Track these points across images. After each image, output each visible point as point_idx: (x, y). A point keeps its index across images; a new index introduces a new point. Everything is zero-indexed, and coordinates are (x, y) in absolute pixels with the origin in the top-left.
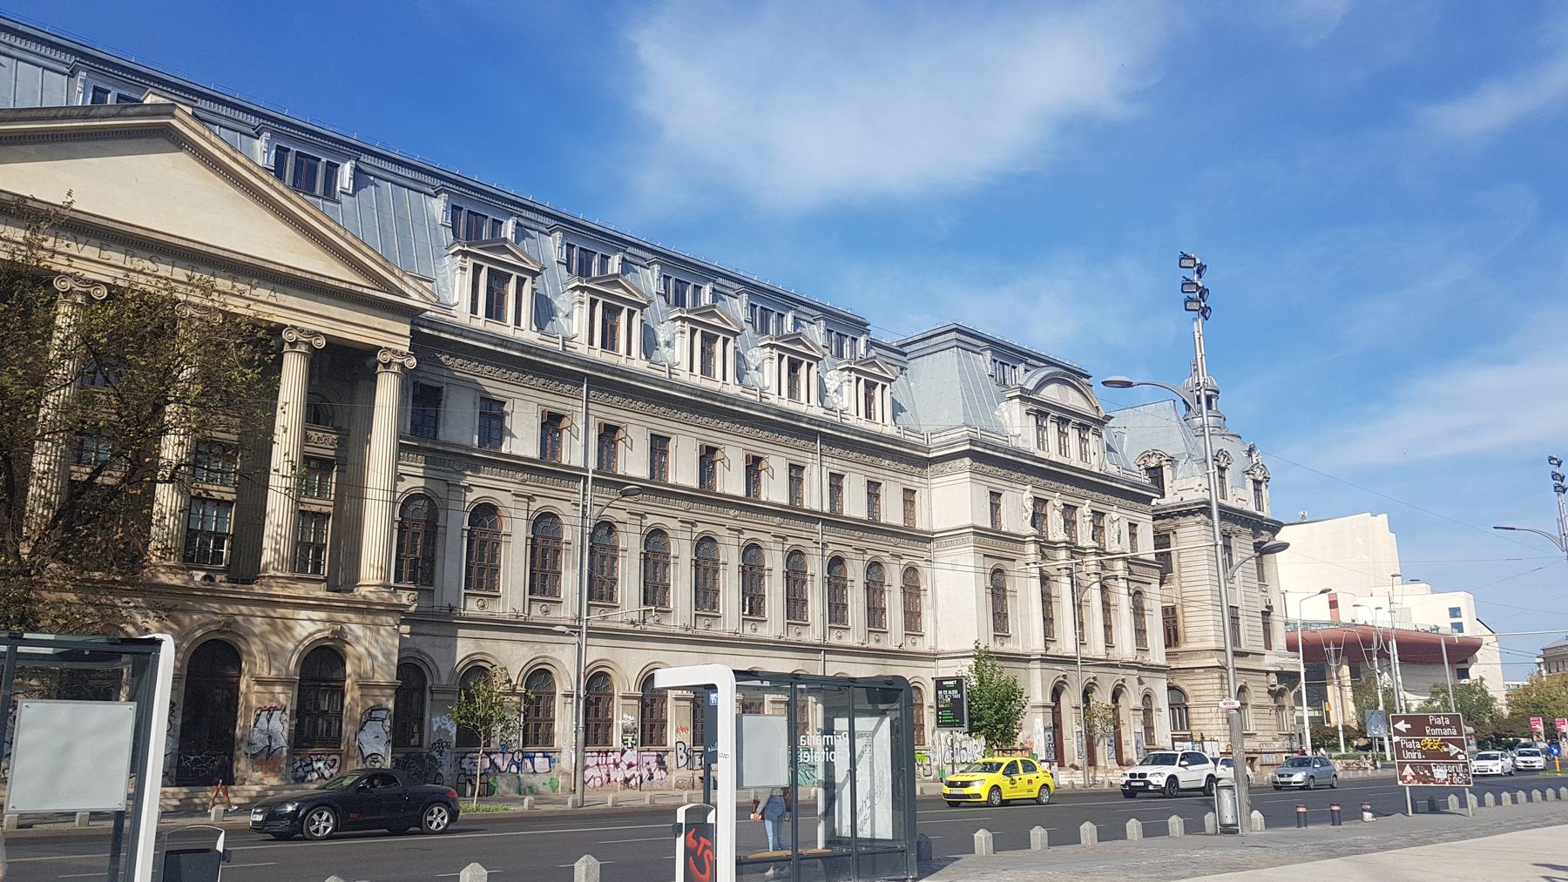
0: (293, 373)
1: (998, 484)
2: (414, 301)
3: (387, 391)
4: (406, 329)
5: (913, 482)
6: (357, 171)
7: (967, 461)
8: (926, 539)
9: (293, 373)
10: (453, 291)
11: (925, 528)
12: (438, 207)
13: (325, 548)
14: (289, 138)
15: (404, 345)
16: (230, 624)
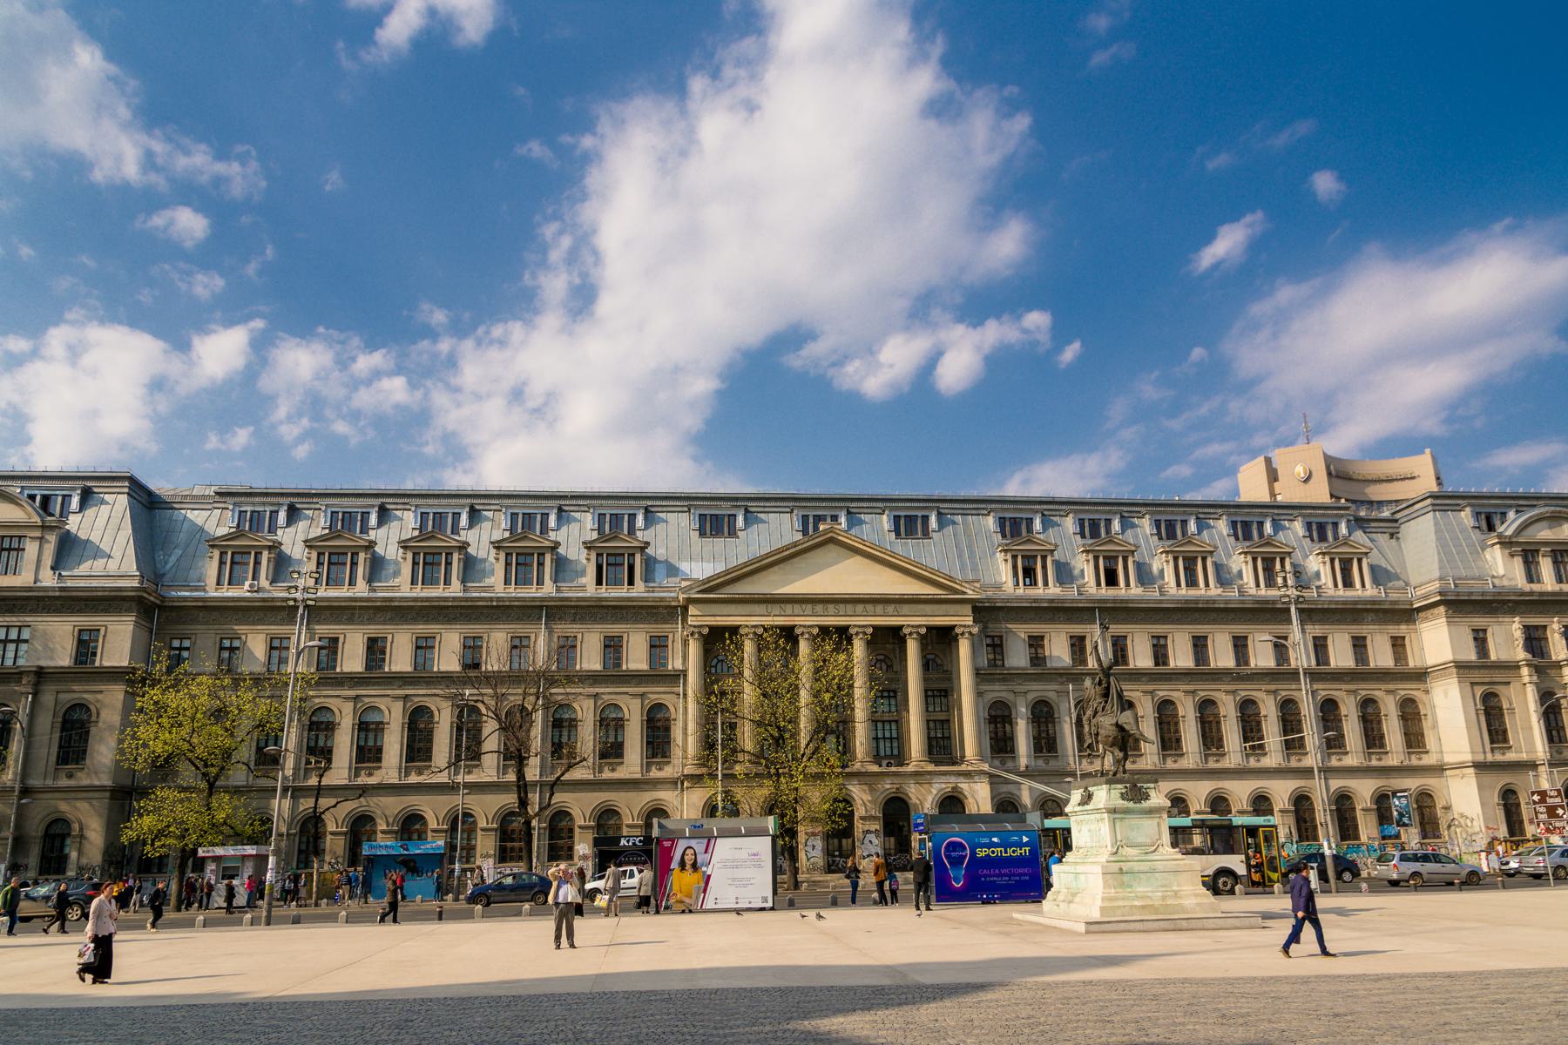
0: (912, 648)
1: (1479, 621)
2: (971, 595)
3: (964, 648)
4: (968, 609)
5: (1402, 629)
6: (939, 514)
7: (1442, 609)
8: (1421, 675)
9: (912, 648)
10: (1002, 576)
11: (1419, 664)
12: (990, 522)
13: (942, 746)
14: (897, 508)
15: (969, 621)
16: (955, 789)
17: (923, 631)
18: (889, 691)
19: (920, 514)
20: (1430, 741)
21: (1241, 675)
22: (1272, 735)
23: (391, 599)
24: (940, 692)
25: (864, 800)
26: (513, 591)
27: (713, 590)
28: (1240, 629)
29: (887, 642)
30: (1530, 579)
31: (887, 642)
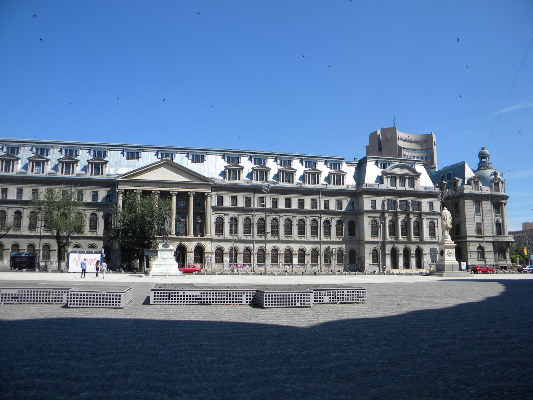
0: (192, 199)
9: (192, 199)
17: (194, 194)
18: (182, 212)
19: (201, 154)
20: (357, 233)
21: (327, 212)
22: (321, 231)
23: (24, 177)
24: (200, 213)
25: (210, 247)
26: (64, 175)
27: (128, 179)
28: (301, 197)
29: (183, 197)
30: (391, 185)
31: (183, 197)
